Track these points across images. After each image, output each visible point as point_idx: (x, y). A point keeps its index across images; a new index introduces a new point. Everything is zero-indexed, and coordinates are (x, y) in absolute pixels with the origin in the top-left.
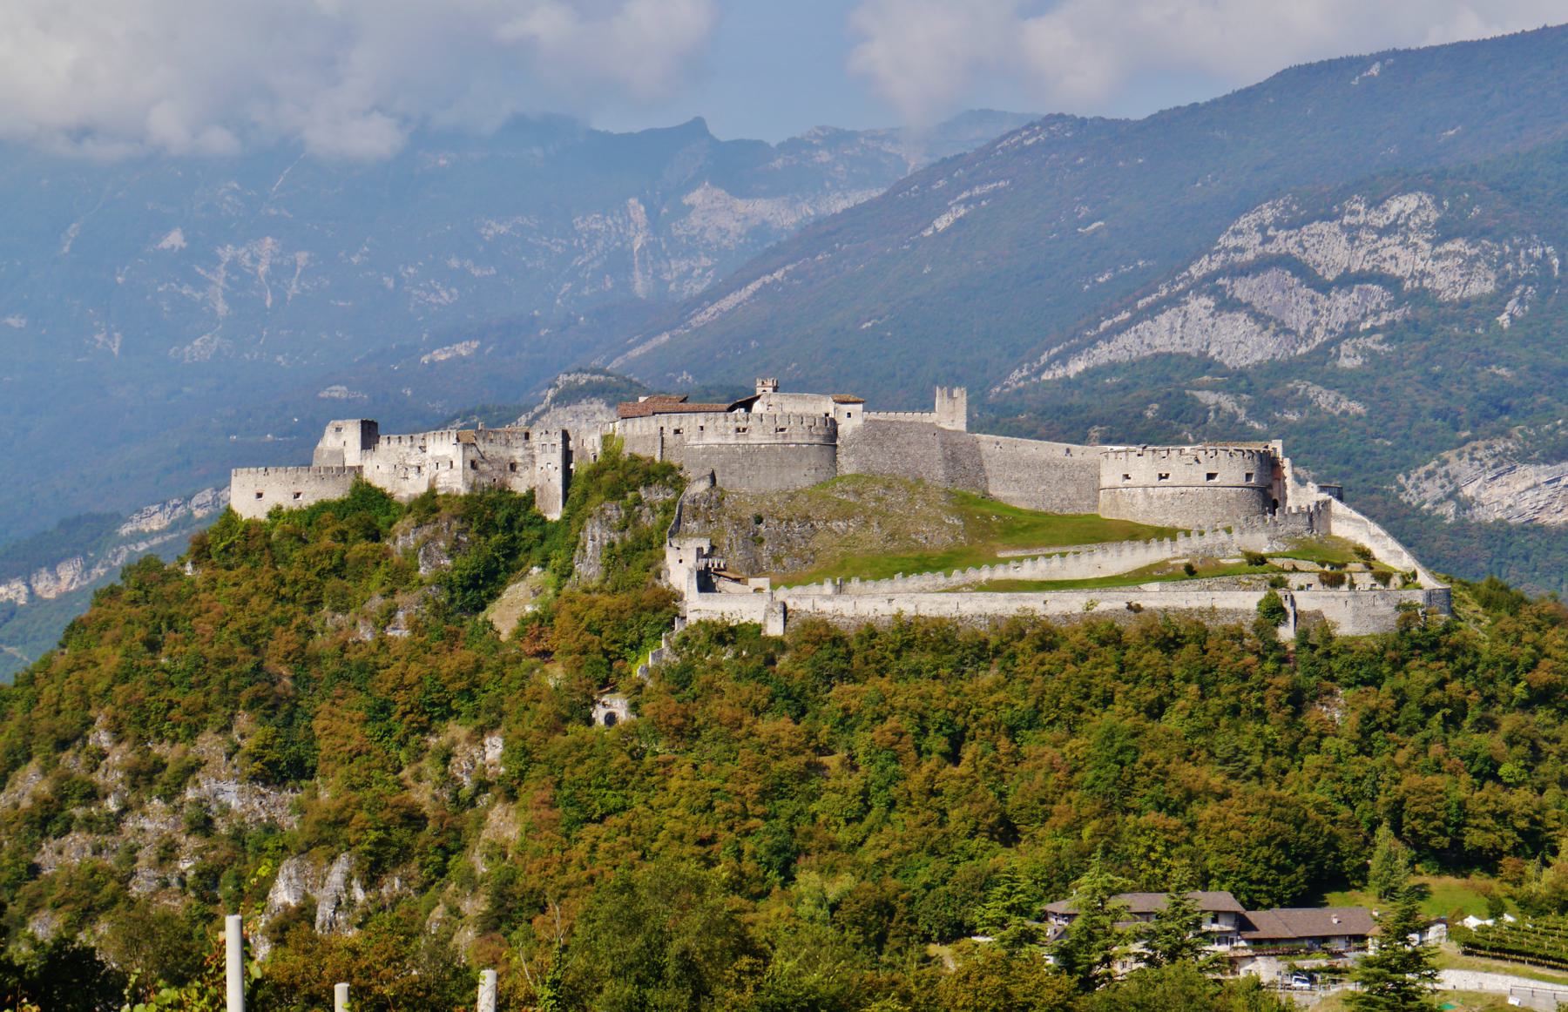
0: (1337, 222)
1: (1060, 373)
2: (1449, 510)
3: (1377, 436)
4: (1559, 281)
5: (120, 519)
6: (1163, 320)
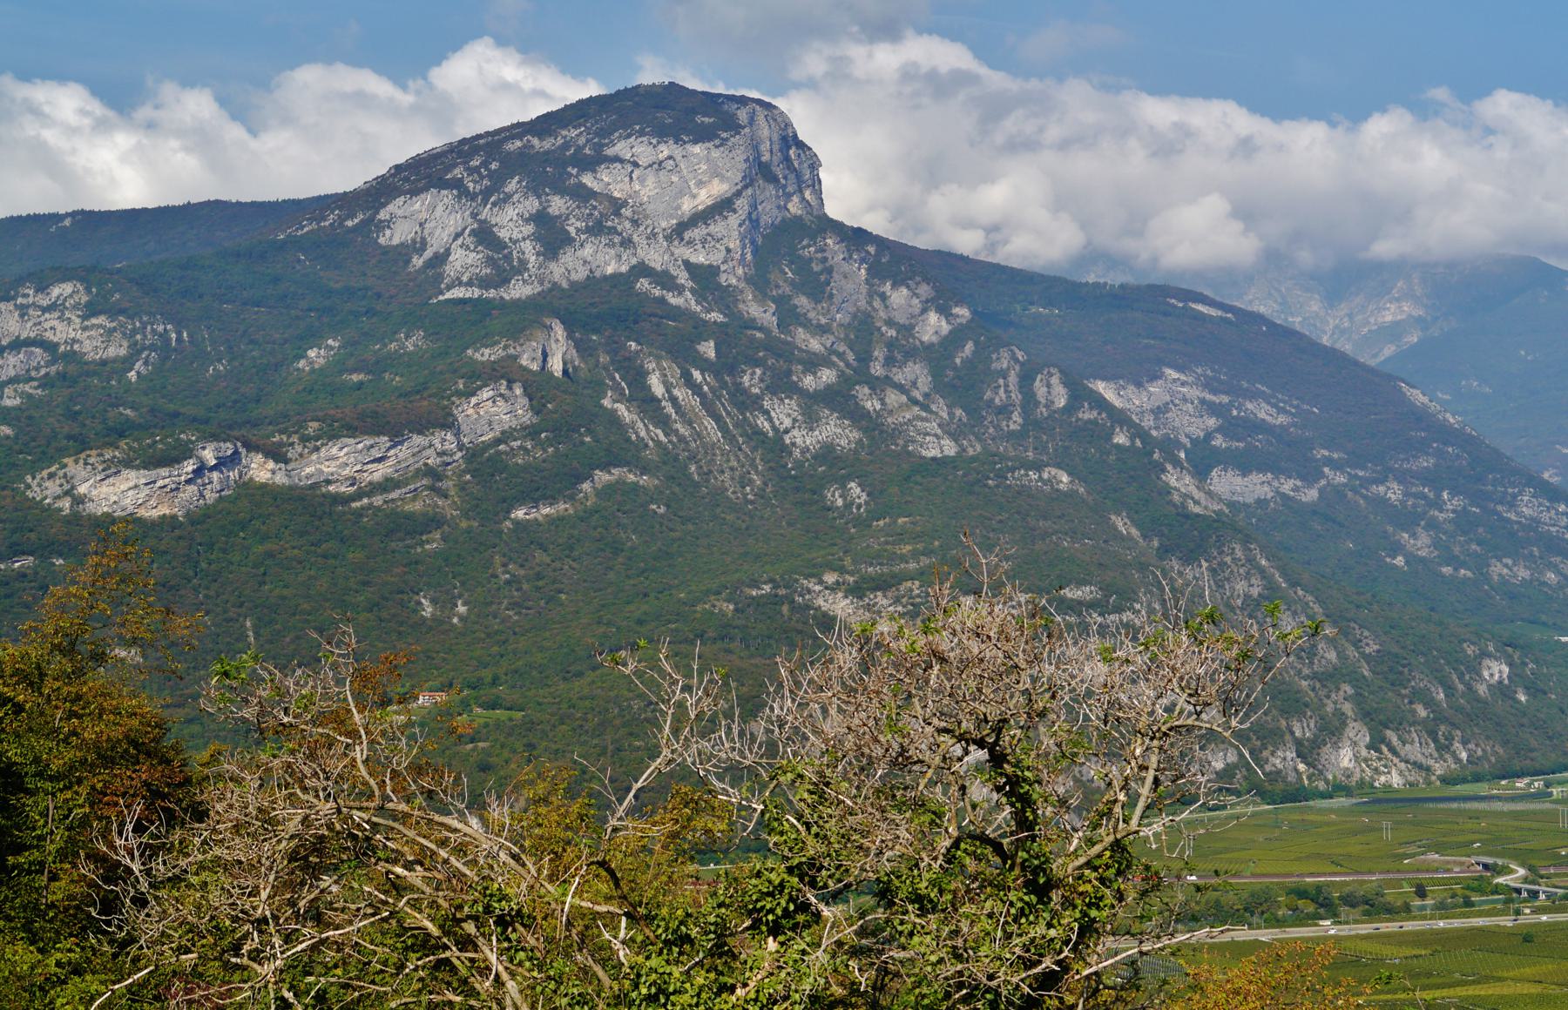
0: (12, 302)
2: (66, 504)
3: (21, 452)
4: (175, 350)
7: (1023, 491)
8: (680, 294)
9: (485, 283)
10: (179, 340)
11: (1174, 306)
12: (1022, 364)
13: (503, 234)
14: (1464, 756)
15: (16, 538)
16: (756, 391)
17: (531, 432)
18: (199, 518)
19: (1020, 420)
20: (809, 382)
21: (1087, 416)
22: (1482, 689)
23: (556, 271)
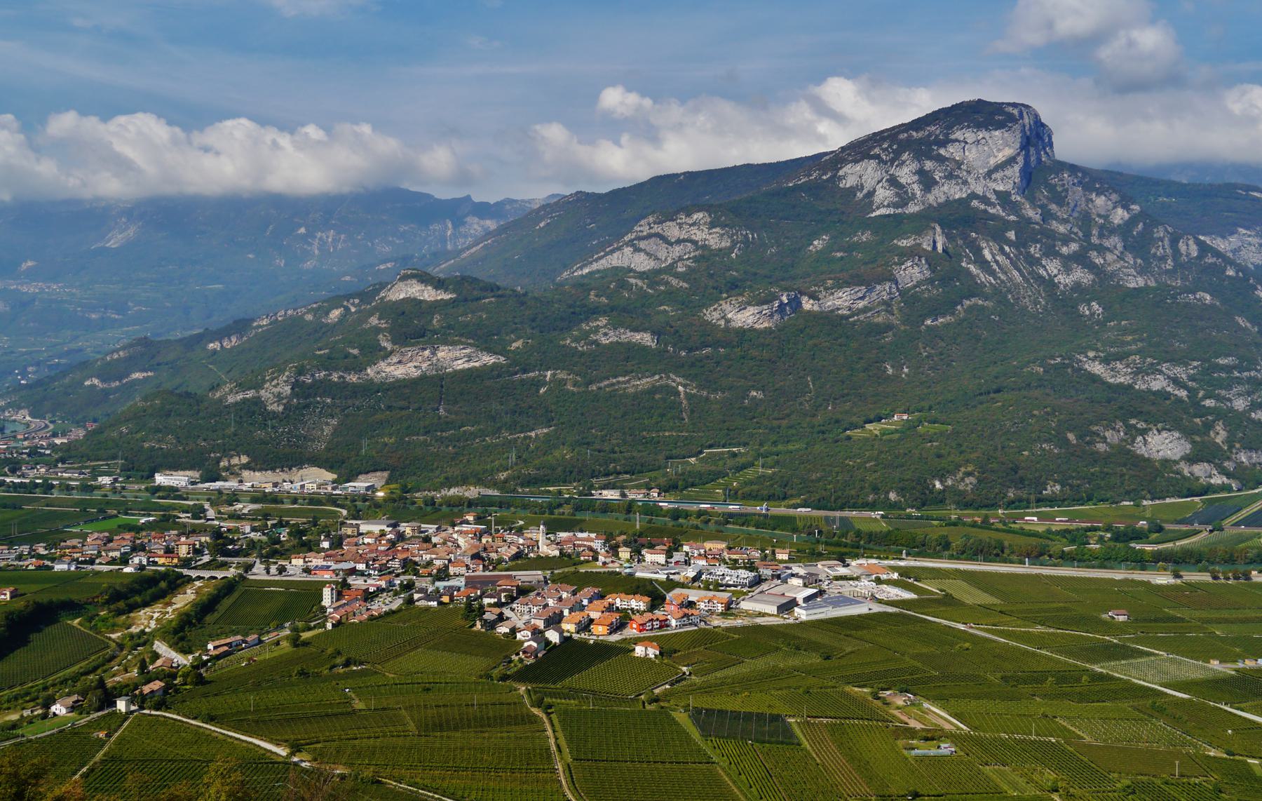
1: (580, 273)
2: (722, 322)
4: (752, 243)
5: (253, 320)
6: (615, 255)
7: (1187, 305)
8: (994, 207)
9: (896, 206)
10: (753, 238)
11: (1242, 194)
12: (1171, 234)
13: (903, 181)
15: (702, 339)
16: (1037, 255)
17: (930, 281)
18: (781, 329)
19: (1172, 264)
20: (1065, 250)
21: (1210, 261)
23: (931, 198)
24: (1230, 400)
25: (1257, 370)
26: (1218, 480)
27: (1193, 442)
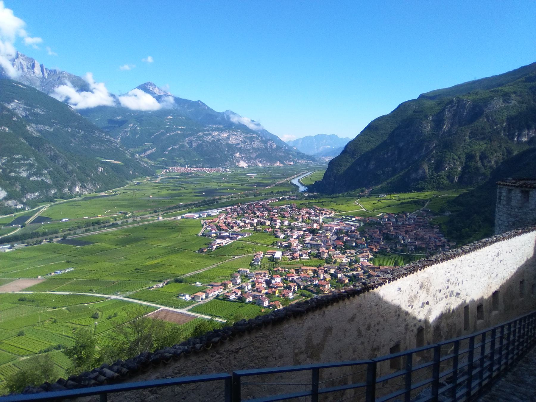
14: (98, 187)
22: (99, 173)
24: (21, 173)
25: (30, 160)
26: (19, 206)
27: (7, 191)
